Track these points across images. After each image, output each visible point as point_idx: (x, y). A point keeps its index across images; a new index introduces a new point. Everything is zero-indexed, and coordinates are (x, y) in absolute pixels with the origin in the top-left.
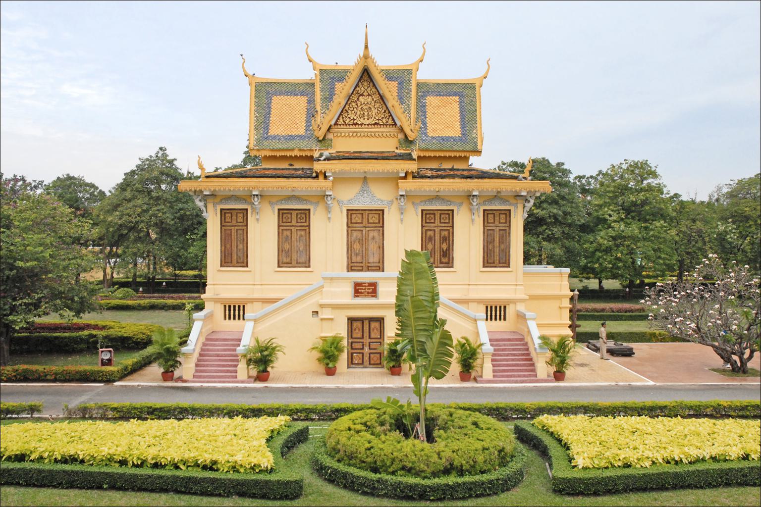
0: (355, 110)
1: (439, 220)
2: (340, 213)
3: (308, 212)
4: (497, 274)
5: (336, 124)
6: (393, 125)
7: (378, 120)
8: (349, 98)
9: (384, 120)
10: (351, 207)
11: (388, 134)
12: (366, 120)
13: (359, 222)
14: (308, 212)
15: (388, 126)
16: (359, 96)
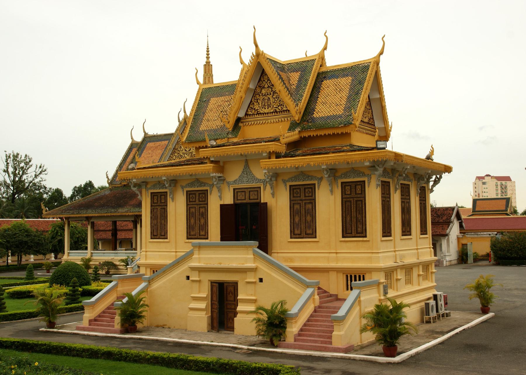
0: (259, 101)
1: (304, 195)
2: (228, 190)
3: (206, 191)
4: (353, 243)
5: (246, 114)
6: (286, 111)
7: (276, 108)
8: (255, 92)
9: (280, 108)
10: (237, 186)
11: (283, 119)
12: (267, 109)
13: (242, 199)
14: (206, 191)
15: (283, 112)
16: (261, 89)
